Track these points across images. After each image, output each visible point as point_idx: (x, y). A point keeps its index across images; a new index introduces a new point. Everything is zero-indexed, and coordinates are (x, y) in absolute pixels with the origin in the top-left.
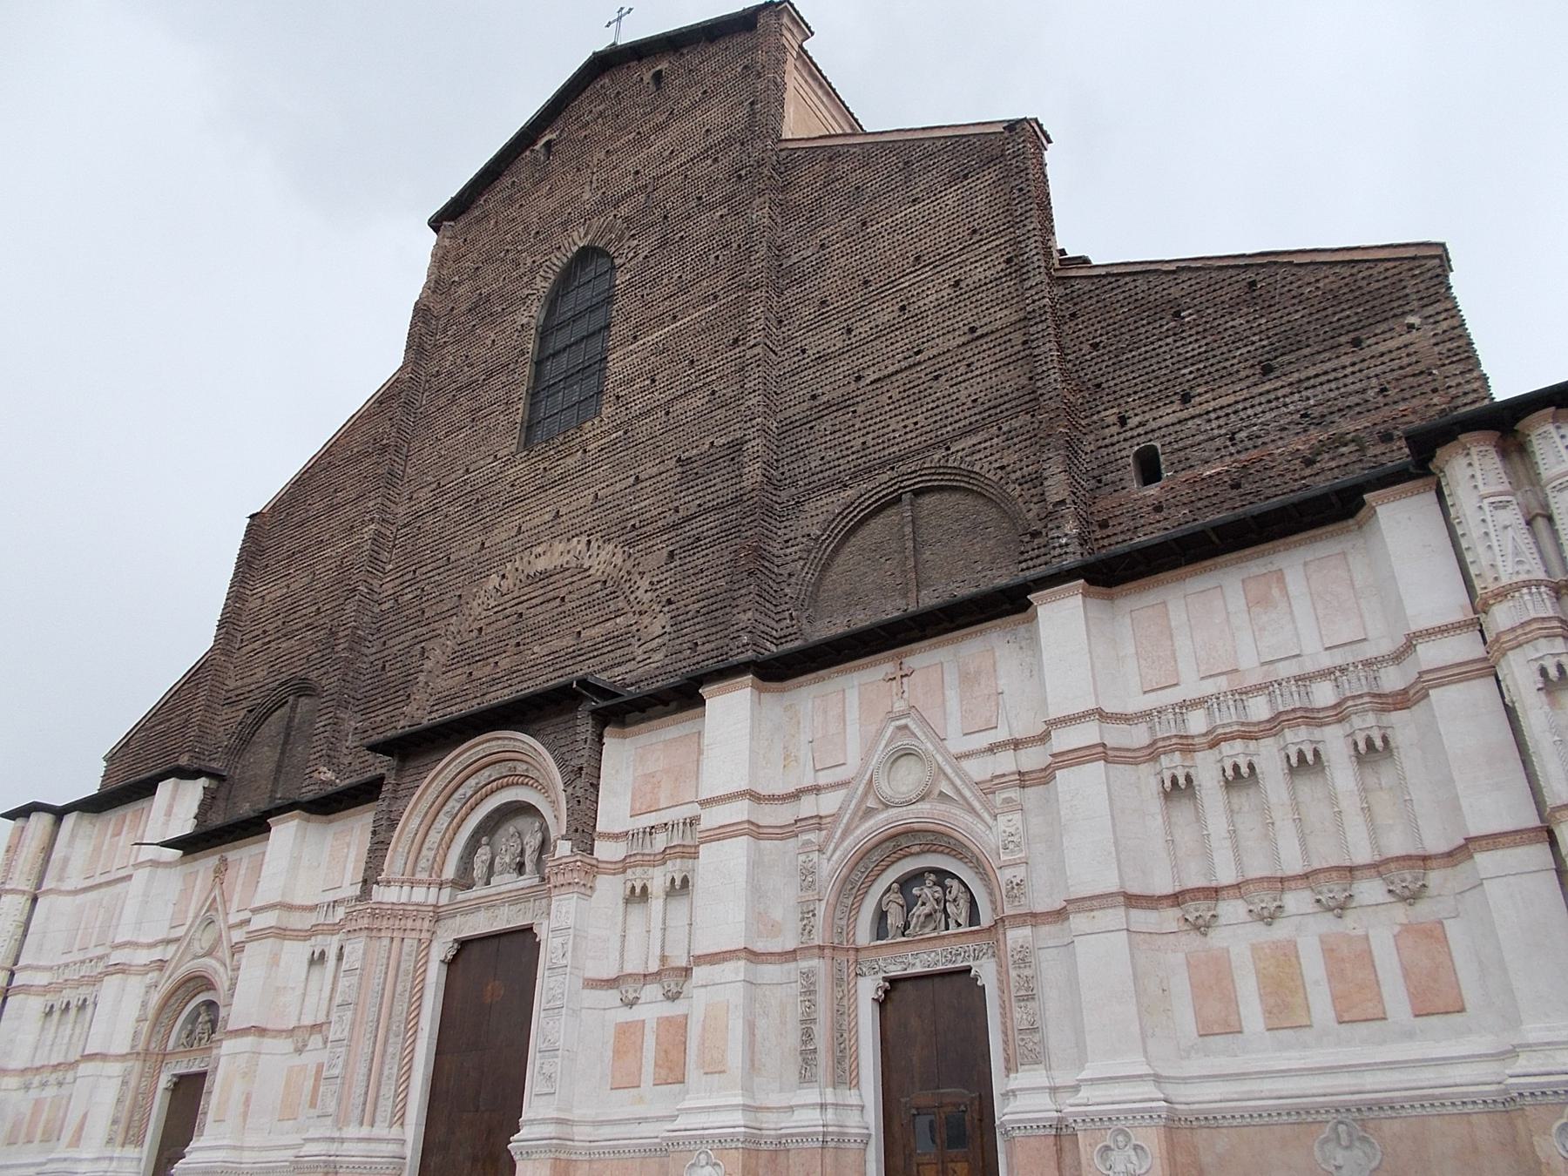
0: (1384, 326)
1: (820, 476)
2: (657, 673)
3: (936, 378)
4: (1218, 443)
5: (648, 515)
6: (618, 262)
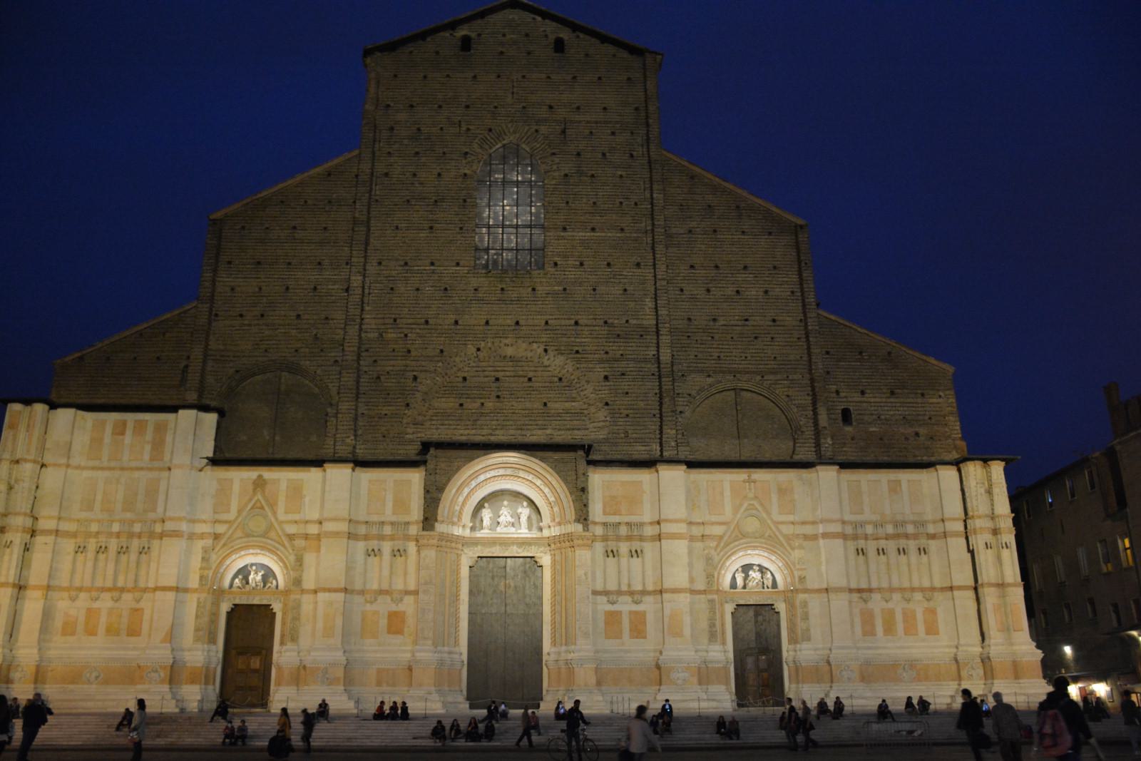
0: (931, 392)
1: (695, 365)
2: (604, 441)
3: (756, 338)
4: (874, 417)
5: (587, 348)
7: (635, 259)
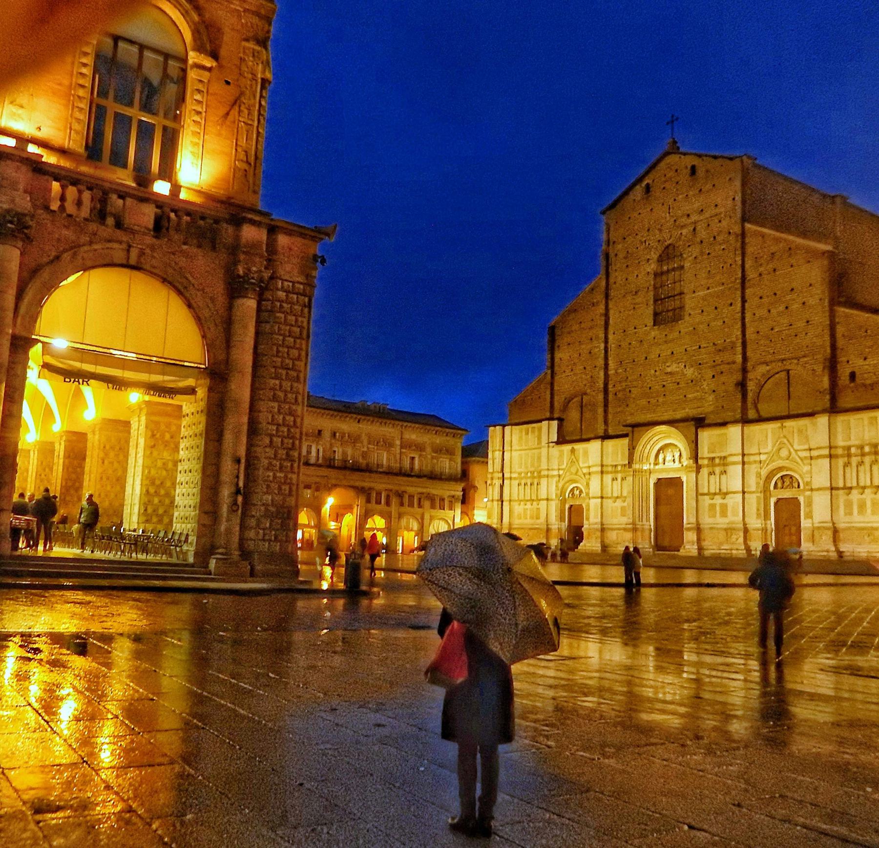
6: (685, 256)
7: (729, 302)
